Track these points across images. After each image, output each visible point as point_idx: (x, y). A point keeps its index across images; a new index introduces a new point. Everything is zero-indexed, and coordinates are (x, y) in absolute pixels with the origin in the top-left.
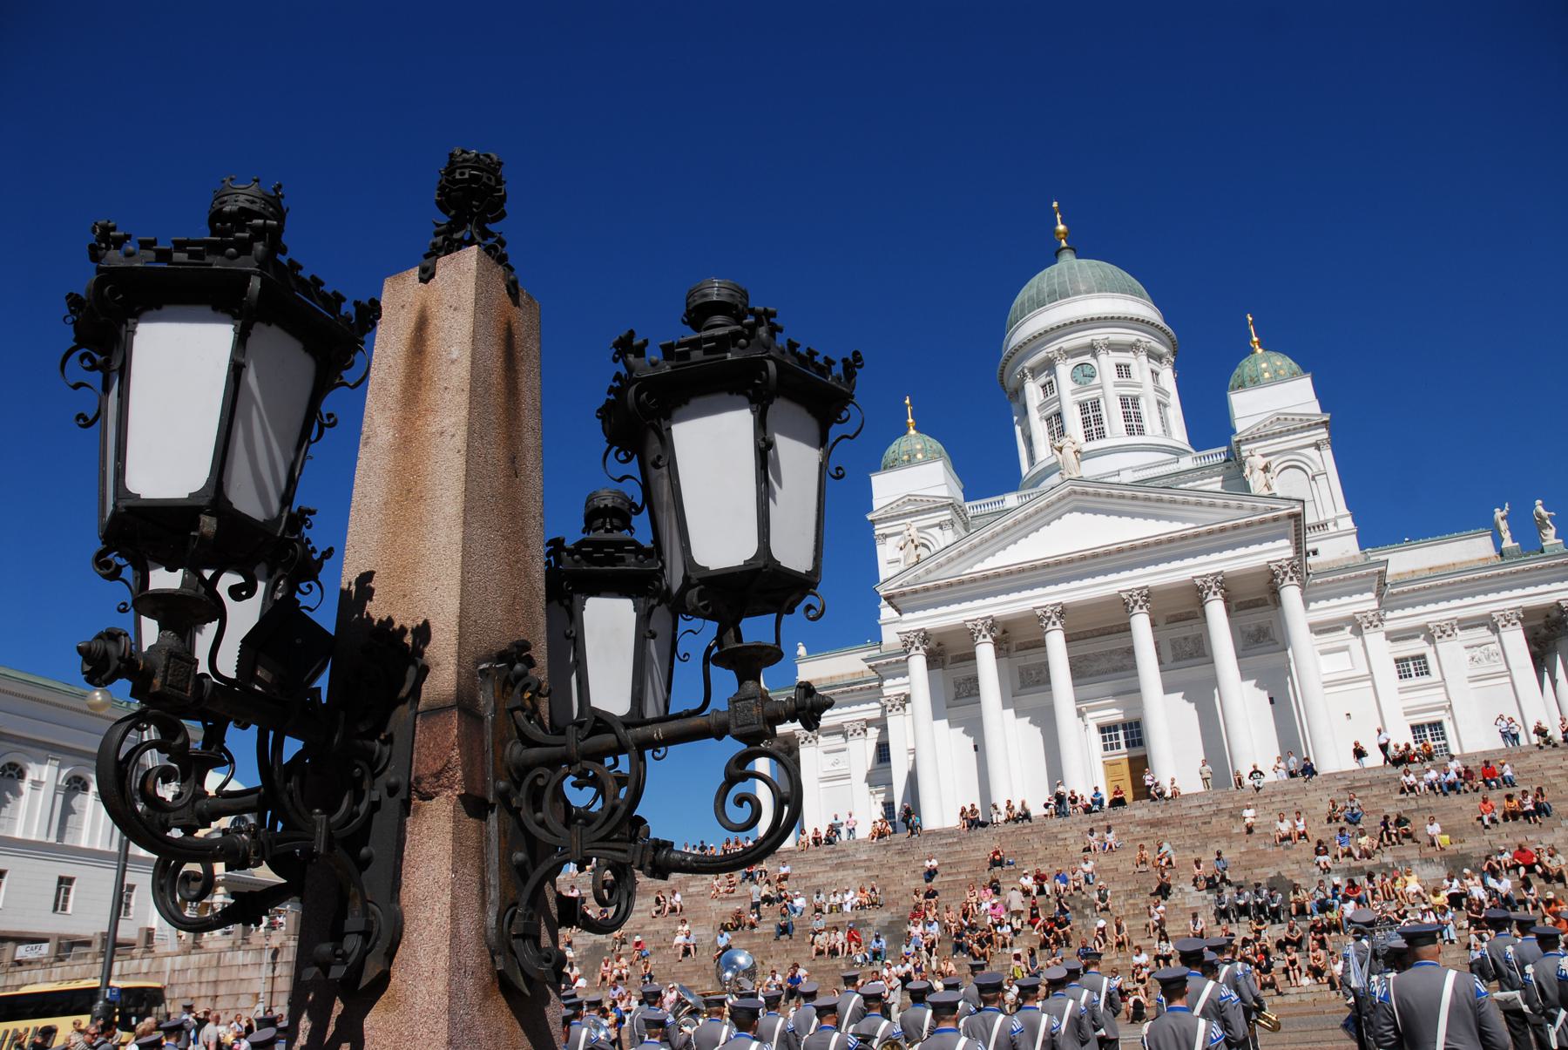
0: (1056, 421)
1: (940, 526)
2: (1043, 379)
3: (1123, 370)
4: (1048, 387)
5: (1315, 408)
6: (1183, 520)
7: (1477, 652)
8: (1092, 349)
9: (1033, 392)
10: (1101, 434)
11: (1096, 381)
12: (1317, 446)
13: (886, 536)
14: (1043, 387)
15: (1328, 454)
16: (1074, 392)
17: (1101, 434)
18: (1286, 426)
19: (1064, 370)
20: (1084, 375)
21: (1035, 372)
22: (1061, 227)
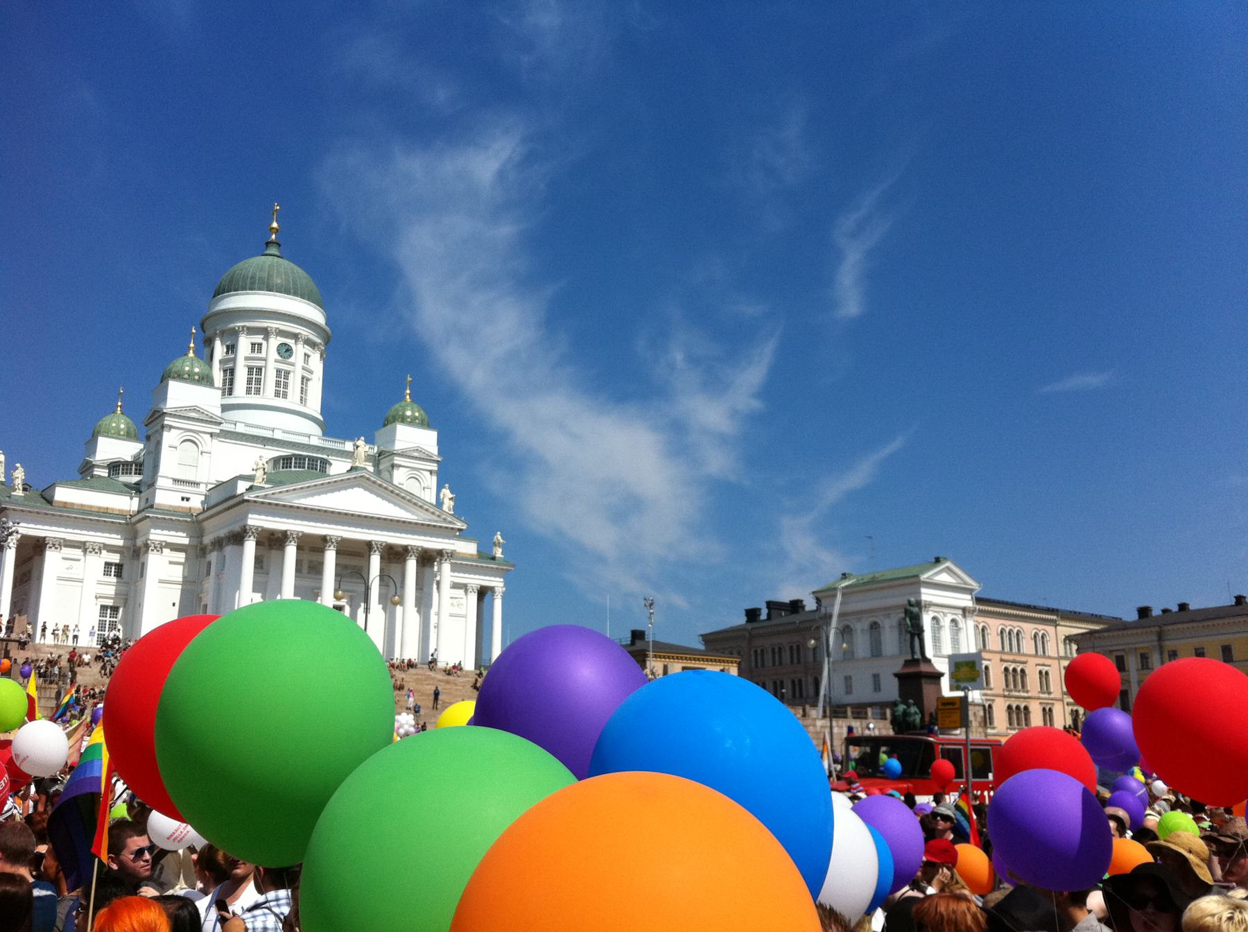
0: (256, 373)
1: (212, 435)
2: (258, 339)
3: (307, 356)
4: (256, 347)
5: (434, 450)
6: (413, 513)
7: (454, 601)
8: (295, 336)
9: (244, 343)
10: (285, 396)
11: (291, 360)
12: (431, 472)
13: (171, 427)
15: (435, 478)
16: (276, 361)
17: (285, 396)
18: (420, 455)
19: (275, 342)
20: (285, 351)
21: (252, 331)
22: (275, 225)
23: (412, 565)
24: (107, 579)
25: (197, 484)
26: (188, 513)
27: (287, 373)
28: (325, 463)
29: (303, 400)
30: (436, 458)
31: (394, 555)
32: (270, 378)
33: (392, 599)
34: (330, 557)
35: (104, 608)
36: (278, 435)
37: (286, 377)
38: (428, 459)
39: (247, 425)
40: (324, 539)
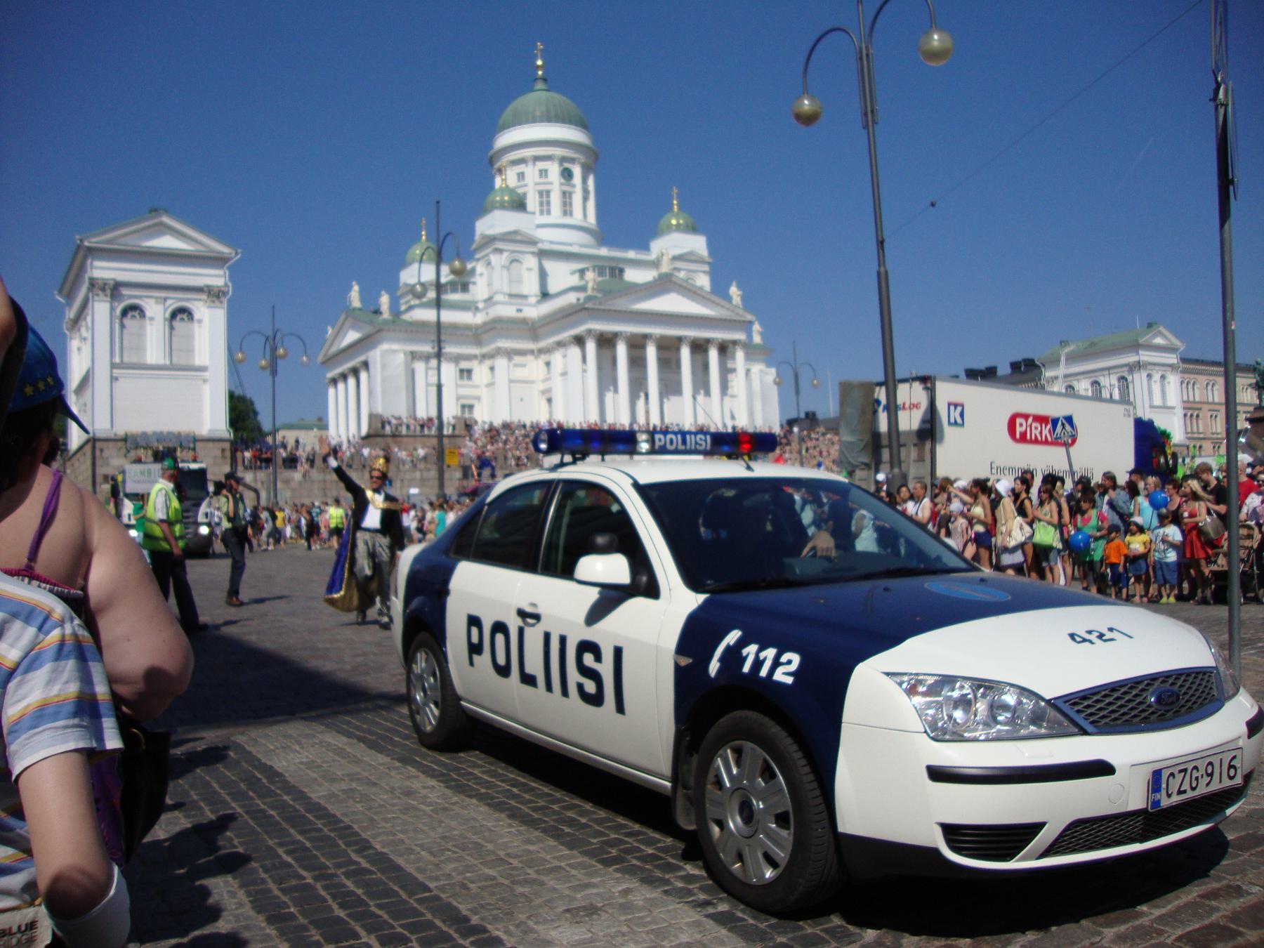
0: (544, 195)
10: (571, 214)
14: (541, 171)
23: (713, 355)
24: (460, 382)
25: (525, 297)
26: (524, 321)
27: (570, 194)
28: (622, 271)
29: (585, 215)
30: (707, 259)
31: (699, 348)
32: (556, 199)
33: (701, 384)
34: (651, 352)
35: (463, 407)
36: (575, 249)
37: (570, 198)
38: (700, 261)
39: (552, 242)
40: (646, 337)
